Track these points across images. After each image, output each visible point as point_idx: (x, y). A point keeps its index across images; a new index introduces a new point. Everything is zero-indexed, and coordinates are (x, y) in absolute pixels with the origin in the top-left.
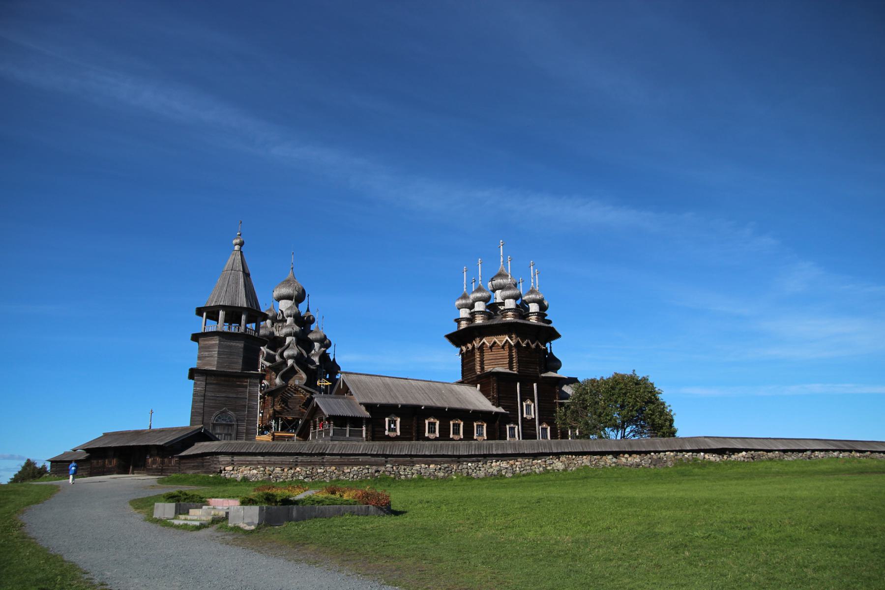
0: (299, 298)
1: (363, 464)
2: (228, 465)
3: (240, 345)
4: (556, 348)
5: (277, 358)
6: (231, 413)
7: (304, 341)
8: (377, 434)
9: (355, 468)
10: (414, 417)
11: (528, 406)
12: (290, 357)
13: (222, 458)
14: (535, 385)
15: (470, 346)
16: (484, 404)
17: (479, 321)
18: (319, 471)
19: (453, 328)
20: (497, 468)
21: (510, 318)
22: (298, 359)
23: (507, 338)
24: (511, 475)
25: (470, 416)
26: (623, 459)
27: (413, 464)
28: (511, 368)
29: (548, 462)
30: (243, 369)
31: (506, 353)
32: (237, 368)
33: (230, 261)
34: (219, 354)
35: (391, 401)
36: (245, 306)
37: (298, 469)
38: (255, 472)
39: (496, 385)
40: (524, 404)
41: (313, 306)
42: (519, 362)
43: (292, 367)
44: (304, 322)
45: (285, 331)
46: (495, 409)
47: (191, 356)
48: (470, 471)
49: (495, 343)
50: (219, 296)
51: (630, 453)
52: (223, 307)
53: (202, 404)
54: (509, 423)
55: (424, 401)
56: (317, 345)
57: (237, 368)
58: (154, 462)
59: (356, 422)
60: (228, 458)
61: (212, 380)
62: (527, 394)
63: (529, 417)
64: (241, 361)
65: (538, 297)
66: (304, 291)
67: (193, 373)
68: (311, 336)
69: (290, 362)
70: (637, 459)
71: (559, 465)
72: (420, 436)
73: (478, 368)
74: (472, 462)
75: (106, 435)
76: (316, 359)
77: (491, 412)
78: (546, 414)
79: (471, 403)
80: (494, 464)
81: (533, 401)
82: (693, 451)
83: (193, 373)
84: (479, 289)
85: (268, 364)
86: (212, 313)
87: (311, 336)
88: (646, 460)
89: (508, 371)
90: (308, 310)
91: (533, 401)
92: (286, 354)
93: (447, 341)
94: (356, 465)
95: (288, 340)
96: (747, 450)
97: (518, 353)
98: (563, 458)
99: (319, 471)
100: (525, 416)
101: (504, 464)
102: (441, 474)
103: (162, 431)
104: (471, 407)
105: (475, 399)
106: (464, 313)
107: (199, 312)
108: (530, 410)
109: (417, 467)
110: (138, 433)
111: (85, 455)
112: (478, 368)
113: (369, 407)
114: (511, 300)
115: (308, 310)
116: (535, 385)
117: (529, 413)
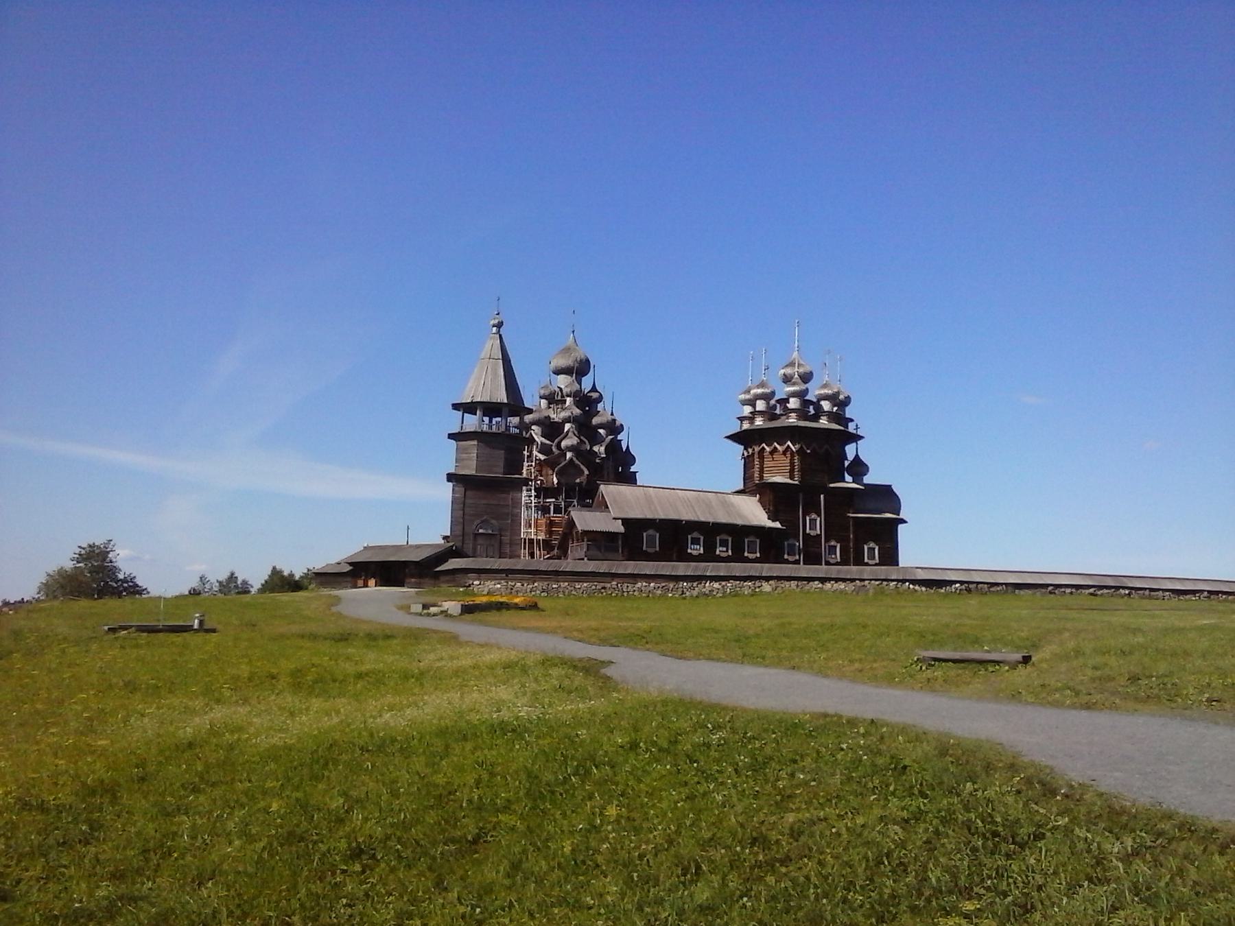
0: (581, 369)
5: (554, 449)
6: (493, 521)
7: (585, 427)
11: (813, 521)
15: (750, 450)
17: (759, 422)
19: (735, 428)
21: (792, 420)
26: (828, 585)
28: (792, 478)
32: (498, 473)
35: (649, 516)
39: (777, 499)
41: (600, 378)
42: (802, 470)
43: (571, 459)
44: (588, 402)
45: (564, 414)
46: (770, 524)
47: (447, 458)
51: (837, 580)
55: (686, 515)
62: (812, 507)
63: (813, 533)
64: (502, 464)
67: (451, 477)
69: (569, 455)
70: (842, 586)
71: (766, 587)
73: (756, 475)
77: (762, 528)
79: (741, 516)
81: (819, 515)
82: (898, 581)
83: (451, 477)
84: (762, 385)
85: (542, 457)
86: (468, 408)
87: (596, 421)
88: (850, 587)
91: (819, 515)
92: (563, 444)
93: (730, 442)
95: (567, 426)
96: (962, 583)
97: (801, 462)
100: (808, 531)
101: (716, 585)
102: (659, 592)
104: (739, 522)
105: (753, 512)
106: (747, 410)
107: (456, 407)
108: (815, 525)
110: (398, 548)
112: (756, 475)
113: (625, 522)
117: (813, 527)
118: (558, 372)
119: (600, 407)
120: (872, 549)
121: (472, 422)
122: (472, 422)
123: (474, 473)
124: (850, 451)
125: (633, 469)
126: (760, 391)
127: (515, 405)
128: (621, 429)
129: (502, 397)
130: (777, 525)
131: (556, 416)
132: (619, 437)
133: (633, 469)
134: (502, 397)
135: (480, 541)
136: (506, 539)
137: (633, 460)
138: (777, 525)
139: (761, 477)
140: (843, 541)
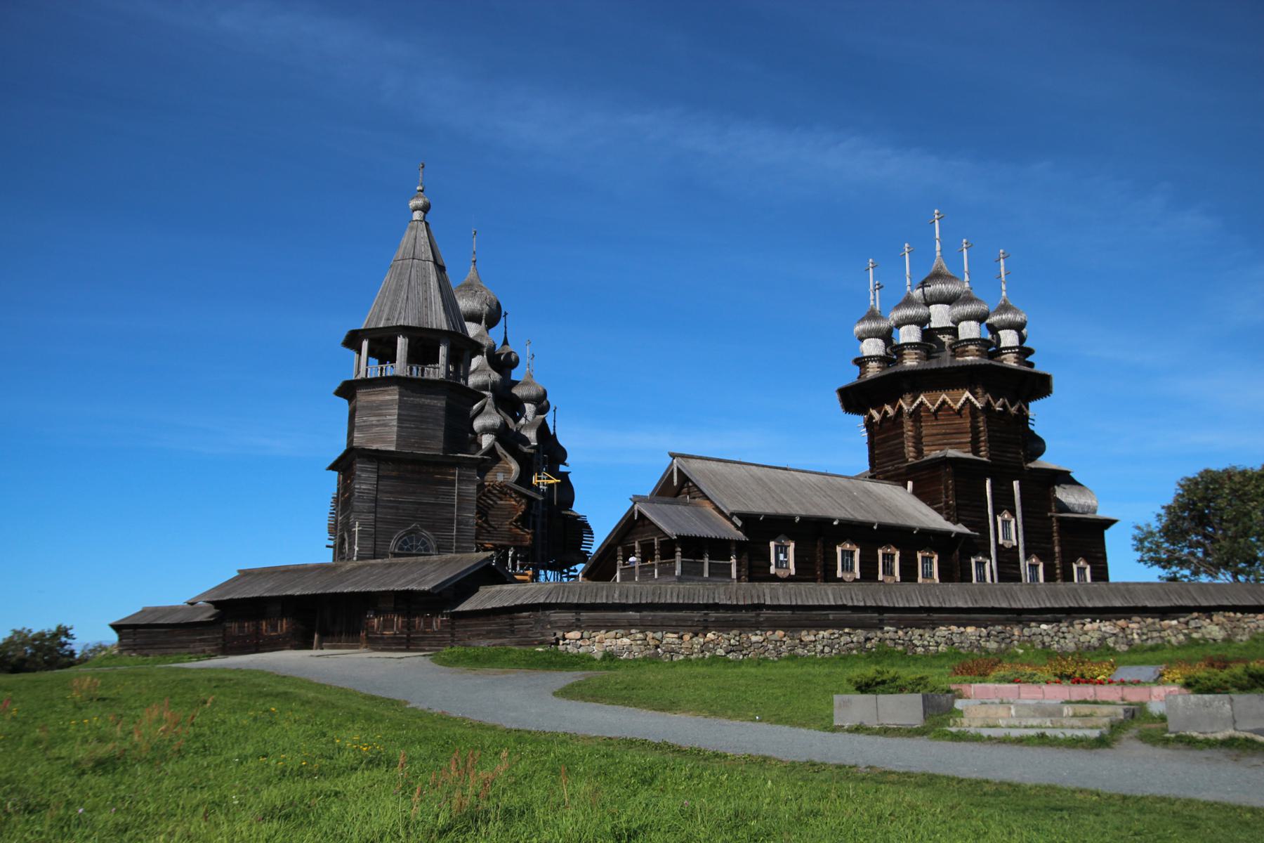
1: (839, 625)
2: (570, 628)
3: (440, 403)
4: (1041, 415)
6: (425, 533)
8: (757, 570)
9: (826, 634)
10: (817, 538)
11: (1006, 523)
12: (486, 430)
13: (555, 616)
14: (1016, 484)
16: (929, 518)
18: (754, 639)
19: (851, 376)
20: (1097, 635)
21: (971, 358)
22: (502, 434)
23: (967, 394)
24: (1125, 648)
25: (909, 540)
27: (934, 626)
28: (976, 451)
29: (1193, 624)
30: (445, 450)
31: (967, 422)
32: (435, 447)
33: (407, 240)
34: (400, 420)
35: (782, 510)
36: (445, 327)
37: (710, 636)
38: (626, 641)
40: (999, 519)
42: (990, 440)
43: (492, 450)
48: (1047, 639)
49: (944, 402)
50: (393, 309)
52: (405, 330)
53: (372, 516)
54: (975, 555)
56: (529, 408)
57: (435, 447)
58: (387, 625)
59: (719, 548)
60: (569, 616)
62: (1003, 502)
63: (1008, 544)
65: (1018, 318)
66: (498, 305)
68: (518, 391)
69: (486, 441)
72: (829, 576)
73: (910, 450)
74: (1047, 622)
75: (244, 574)
76: (531, 435)
77: (949, 533)
78: (1036, 541)
80: (1088, 626)
81: (1013, 514)
86: (382, 344)
89: (970, 456)
90: (506, 343)
91: (1013, 514)
94: (825, 628)
97: (988, 422)
98: (1217, 617)
99: (754, 639)
100: (1001, 541)
101: (1107, 627)
106: (873, 347)
107: (353, 340)
108: (1009, 530)
109: (942, 631)
112: (910, 450)
113: (749, 521)
114: (973, 323)
115: (506, 343)
116: (1016, 484)
120: (1082, 568)
123: (393, 449)
124: (1041, 415)
126: (867, 325)
130: (960, 528)
138: (960, 528)
139: (919, 452)
140: (1046, 556)
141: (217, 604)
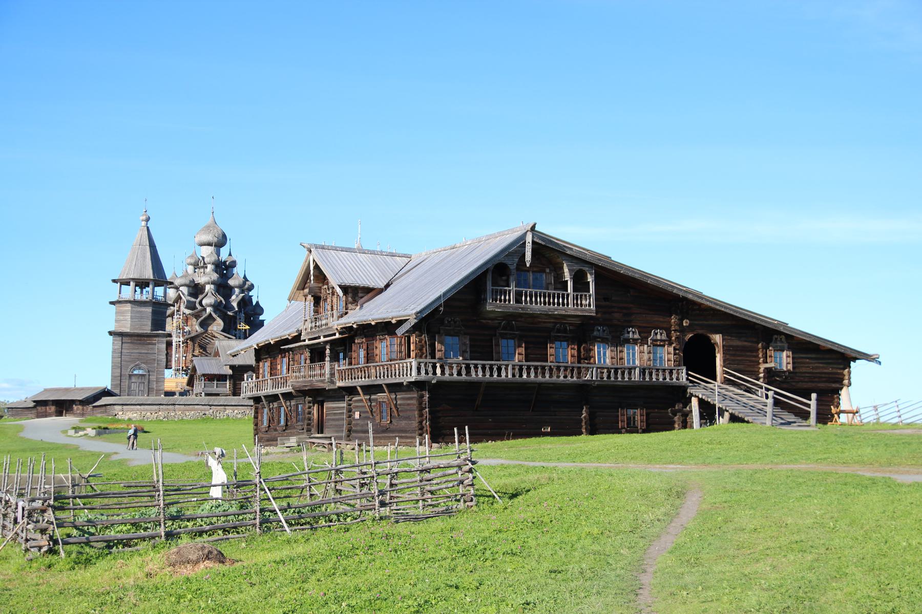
0: (221, 242)
3: (149, 310)
5: (197, 305)
7: (223, 288)
13: (116, 407)
22: (217, 307)
30: (152, 330)
32: (147, 329)
36: (152, 277)
44: (224, 269)
47: (109, 319)
50: (130, 269)
52: (133, 279)
56: (237, 290)
57: (147, 329)
58: (78, 409)
59: (221, 378)
60: (120, 407)
61: (126, 339)
64: (150, 323)
66: (224, 236)
68: (231, 282)
69: (209, 310)
75: (46, 390)
76: (235, 304)
85: (188, 312)
87: (231, 282)
90: (230, 255)
92: (204, 302)
102: (239, 416)
103: (82, 389)
110: (67, 390)
111: (32, 404)
113: (232, 367)
115: (230, 255)
118: (202, 245)
119: (235, 270)
121: (128, 292)
122: (128, 292)
125: (261, 318)
127: (160, 280)
128: (251, 287)
129: (149, 274)
131: (201, 279)
132: (251, 294)
133: (261, 318)
134: (149, 274)
135: (133, 380)
136: (153, 378)
137: (261, 311)
141: (34, 401)
